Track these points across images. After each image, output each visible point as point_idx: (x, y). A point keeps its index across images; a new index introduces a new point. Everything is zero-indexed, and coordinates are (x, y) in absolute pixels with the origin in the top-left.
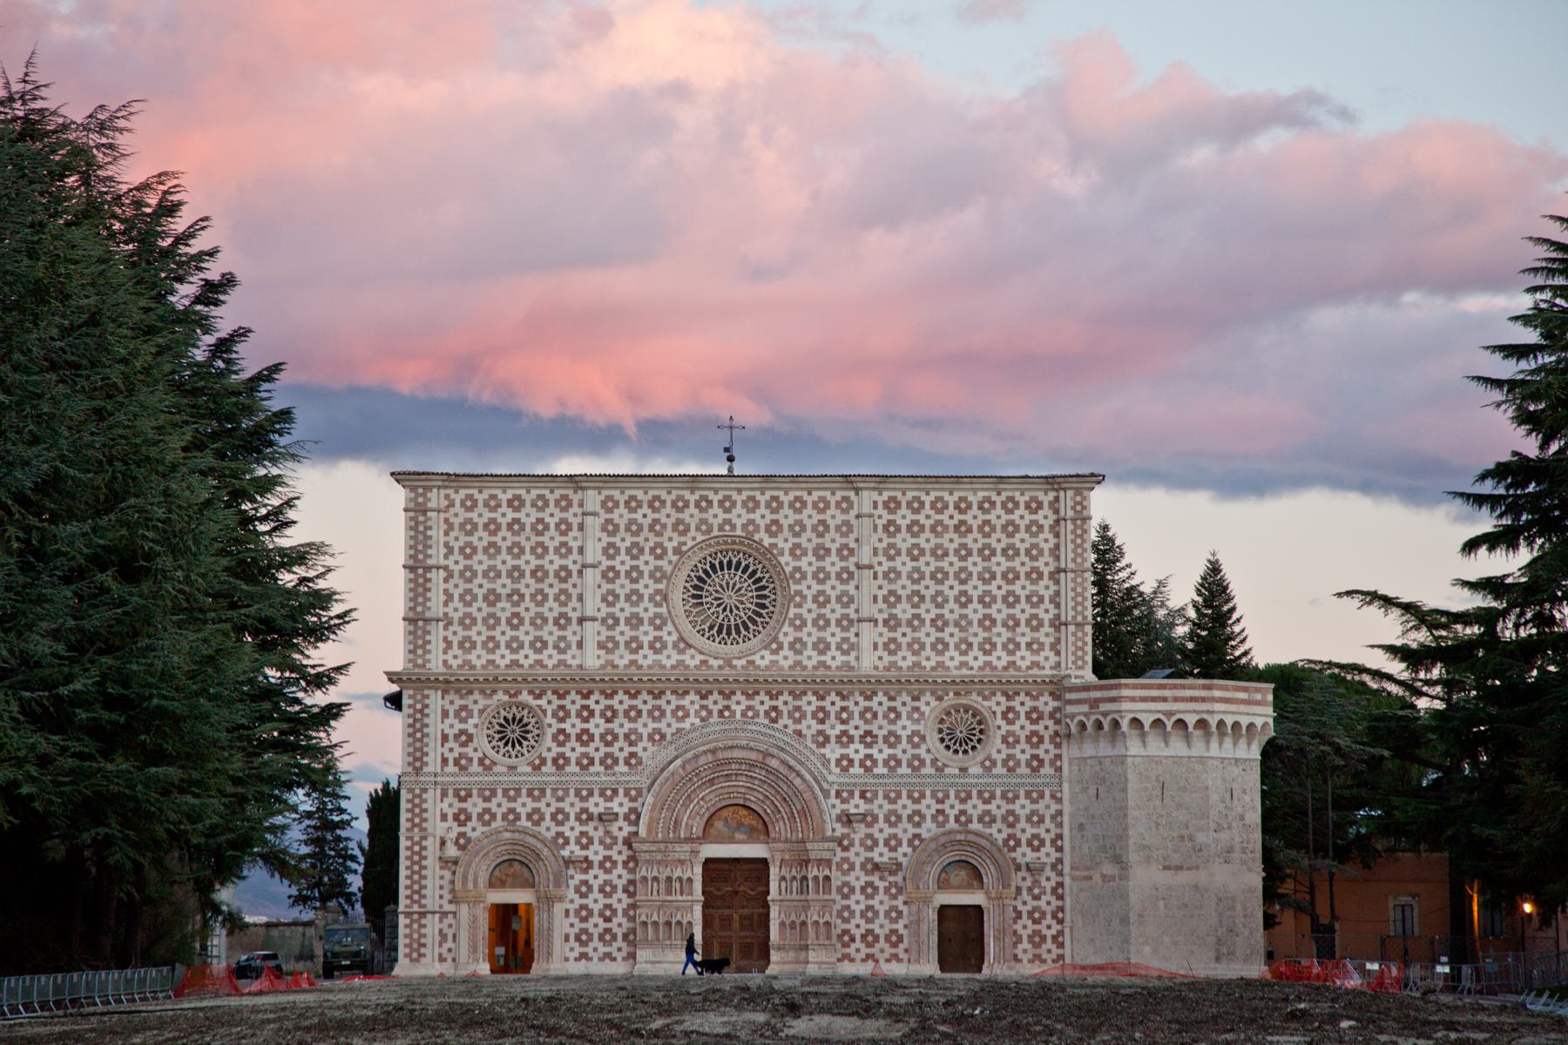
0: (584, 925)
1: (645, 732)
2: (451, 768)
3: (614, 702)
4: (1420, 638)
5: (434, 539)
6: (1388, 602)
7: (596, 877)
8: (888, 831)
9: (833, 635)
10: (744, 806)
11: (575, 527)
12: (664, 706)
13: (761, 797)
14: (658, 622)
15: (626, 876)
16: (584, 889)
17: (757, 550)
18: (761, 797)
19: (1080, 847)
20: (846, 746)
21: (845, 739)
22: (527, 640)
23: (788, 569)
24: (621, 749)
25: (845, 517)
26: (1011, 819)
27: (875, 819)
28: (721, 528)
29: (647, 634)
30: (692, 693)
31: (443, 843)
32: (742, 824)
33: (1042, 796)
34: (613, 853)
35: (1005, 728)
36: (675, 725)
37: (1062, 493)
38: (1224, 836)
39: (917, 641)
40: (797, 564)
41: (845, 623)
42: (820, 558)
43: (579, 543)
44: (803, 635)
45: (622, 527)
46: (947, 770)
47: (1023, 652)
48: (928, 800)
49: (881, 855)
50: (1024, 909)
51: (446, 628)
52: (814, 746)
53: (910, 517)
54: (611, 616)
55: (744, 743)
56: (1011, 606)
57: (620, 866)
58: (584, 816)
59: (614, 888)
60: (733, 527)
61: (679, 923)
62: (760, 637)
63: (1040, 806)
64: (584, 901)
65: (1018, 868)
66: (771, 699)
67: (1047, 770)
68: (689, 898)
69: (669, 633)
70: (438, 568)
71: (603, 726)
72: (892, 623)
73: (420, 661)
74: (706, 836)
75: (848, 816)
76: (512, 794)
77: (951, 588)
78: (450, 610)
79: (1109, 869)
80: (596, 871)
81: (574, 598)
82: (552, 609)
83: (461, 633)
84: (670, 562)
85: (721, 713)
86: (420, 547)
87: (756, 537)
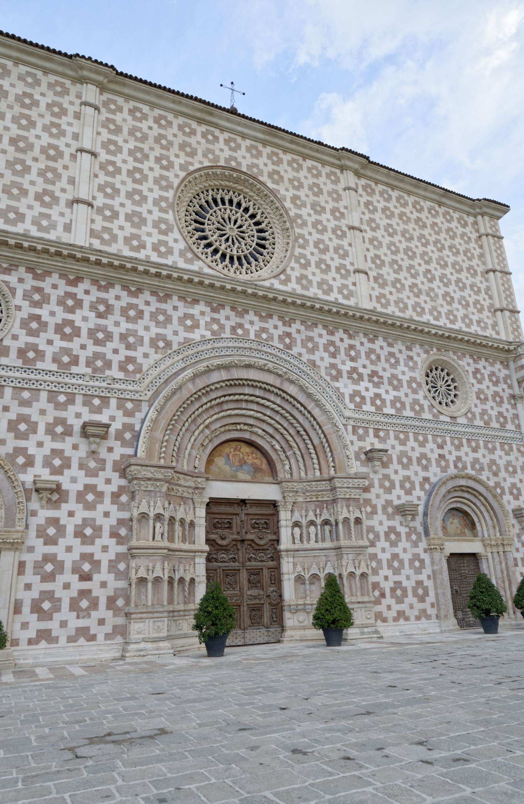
0: (47, 586)
7: (71, 514)
8: (403, 473)
13: (271, 431)
14: (163, 226)
15: (116, 514)
16: (51, 531)
17: (259, 192)
18: (271, 431)
23: (292, 214)
28: (227, 160)
32: (245, 462)
33: (511, 449)
34: (99, 482)
35: (477, 386)
36: (183, 335)
37: (479, 217)
40: (298, 212)
43: (75, 129)
46: (442, 418)
48: (430, 445)
49: (399, 497)
52: (328, 378)
54: (110, 208)
57: (107, 499)
58: (59, 429)
59: (98, 530)
60: (239, 164)
61: (182, 580)
62: (269, 265)
64: (50, 549)
66: (284, 324)
67: (510, 426)
71: (93, 321)
72: (380, 281)
80: (71, 505)
85: (233, 329)
87: (260, 178)
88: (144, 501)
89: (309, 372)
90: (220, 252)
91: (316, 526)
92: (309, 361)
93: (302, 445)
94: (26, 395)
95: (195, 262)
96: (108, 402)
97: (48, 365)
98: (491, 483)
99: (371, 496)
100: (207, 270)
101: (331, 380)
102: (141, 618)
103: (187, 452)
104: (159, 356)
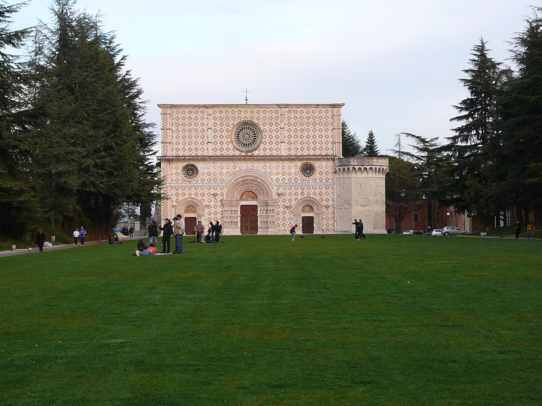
2: (174, 182)
4: (421, 145)
5: (169, 122)
6: (413, 136)
8: (289, 197)
10: (251, 191)
11: (206, 118)
14: (228, 143)
19: (339, 201)
20: (277, 175)
22: (193, 148)
23: (262, 129)
25: (277, 115)
26: (321, 194)
27: (286, 194)
29: (225, 146)
31: (173, 201)
33: (329, 188)
37: (334, 108)
38: (376, 197)
39: (296, 147)
40: (264, 128)
42: (270, 126)
43: (207, 123)
45: (218, 118)
47: (324, 150)
50: (324, 217)
51: (172, 145)
52: (269, 175)
53: (294, 115)
54: (215, 141)
55: (251, 175)
56: (321, 138)
57: (219, 207)
58: (209, 194)
60: (247, 118)
61: (234, 222)
63: (329, 191)
65: (323, 207)
69: (231, 146)
70: (170, 129)
73: (165, 154)
74: (241, 199)
75: (278, 193)
76: (190, 188)
77: (305, 134)
78: (173, 140)
79: (346, 206)
81: (206, 137)
82: (200, 140)
83: (176, 146)
84: (231, 127)
86: (165, 124)
94: (203, 188)
97: (206, 182)
98: (318, 199)
99: (279, 204)
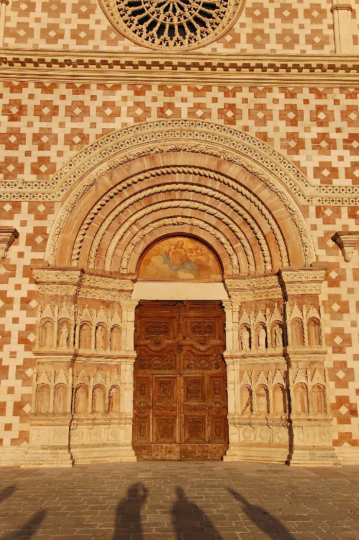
1: (61, 134)
3: (22, 96)
9: (302, 27)
12: (87, 102)
13: (214, 221)
15: (25, 320)
18: (214, 221)
20: (326, 152)
21: (324, 144)
24: (28, 154)
30: (124, 87)
32: (188, 260)
36: (101, 125)
41: (315, 14)
44: (265, 26)
52: (284, 152)
57: (17, 305)
66: (226, 95)
68: (117, 353)
69: (98, 22)
85: (161, 110)
88: (48, 306)
89: (257, 147)
90: (176, 28)
91: (265, 328)
92: (258, 134)
93: (250, 235)
95: (120, 42)
96: (20, 207)
100: (133, 48)
101: (288, 154)
102: (41, 425)
103: (110, 253)
104: (75, 152)
